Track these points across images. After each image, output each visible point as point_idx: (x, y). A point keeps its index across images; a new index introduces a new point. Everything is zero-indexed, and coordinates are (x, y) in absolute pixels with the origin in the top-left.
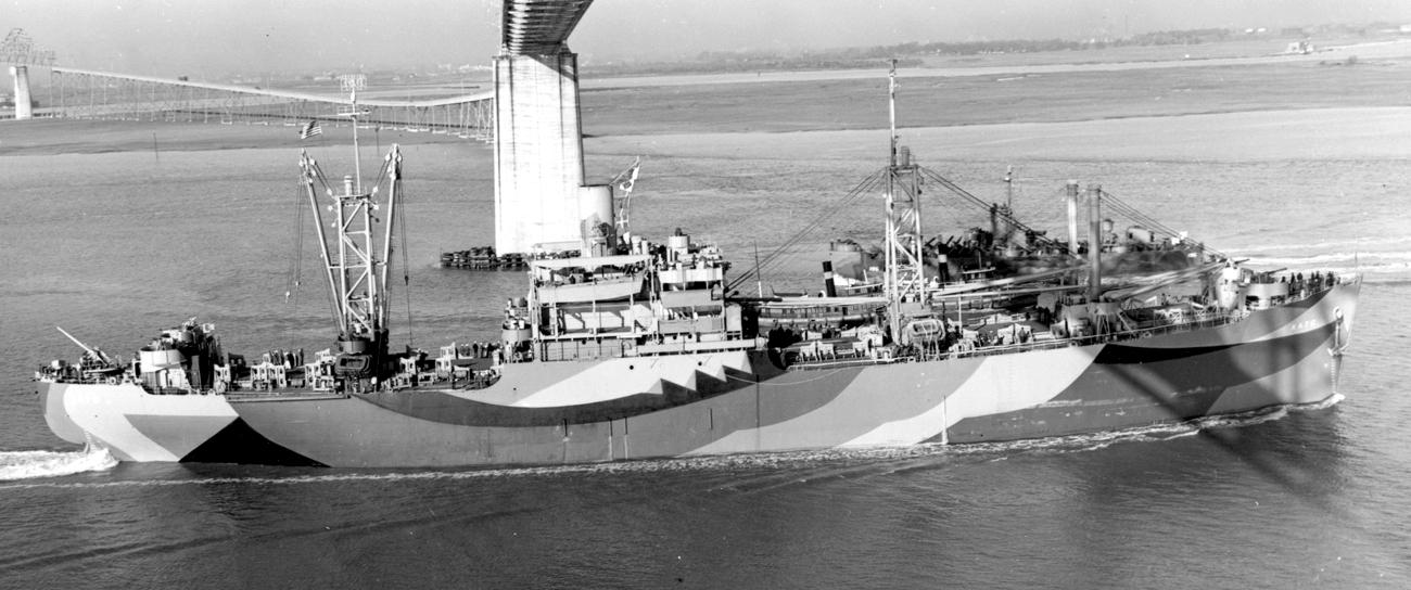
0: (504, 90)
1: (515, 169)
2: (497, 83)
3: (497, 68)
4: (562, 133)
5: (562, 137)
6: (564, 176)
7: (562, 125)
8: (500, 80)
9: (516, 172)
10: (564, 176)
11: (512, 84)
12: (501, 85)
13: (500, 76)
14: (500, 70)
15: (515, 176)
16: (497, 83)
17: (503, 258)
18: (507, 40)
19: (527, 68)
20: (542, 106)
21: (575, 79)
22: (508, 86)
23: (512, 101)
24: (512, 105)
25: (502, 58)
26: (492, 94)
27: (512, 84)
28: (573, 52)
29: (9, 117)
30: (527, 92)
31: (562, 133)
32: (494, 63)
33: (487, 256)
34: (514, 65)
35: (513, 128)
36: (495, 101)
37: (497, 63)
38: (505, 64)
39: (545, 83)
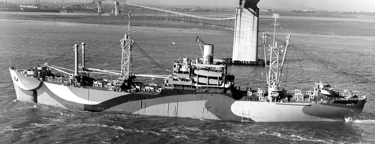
0: (239, 17)
1: (239, 38)
2: (237, 15)
3: (237, 11)
6: (253, 41)
7: (253, 27)
8: (238, 14)
9: (240, 39)
10: (253, 41)
11: (241, 15)
13: (238, 13)
14: (238, 11)
15: (239, 40)
16: (237, 15)
18: (241, 4)
19: (245, 11)
20: (248, 22)
21: (258, 16)
22: (240, 16)
25: (239, 8)
26: (236, 18)
27: (241, 15)
29: (114, 15)
30: (245, 18)
32: (237, 9)
33: (230, 61)
35: (240, 27)
36: (236, 20)
37: (237, 9)
38: (239, 10)
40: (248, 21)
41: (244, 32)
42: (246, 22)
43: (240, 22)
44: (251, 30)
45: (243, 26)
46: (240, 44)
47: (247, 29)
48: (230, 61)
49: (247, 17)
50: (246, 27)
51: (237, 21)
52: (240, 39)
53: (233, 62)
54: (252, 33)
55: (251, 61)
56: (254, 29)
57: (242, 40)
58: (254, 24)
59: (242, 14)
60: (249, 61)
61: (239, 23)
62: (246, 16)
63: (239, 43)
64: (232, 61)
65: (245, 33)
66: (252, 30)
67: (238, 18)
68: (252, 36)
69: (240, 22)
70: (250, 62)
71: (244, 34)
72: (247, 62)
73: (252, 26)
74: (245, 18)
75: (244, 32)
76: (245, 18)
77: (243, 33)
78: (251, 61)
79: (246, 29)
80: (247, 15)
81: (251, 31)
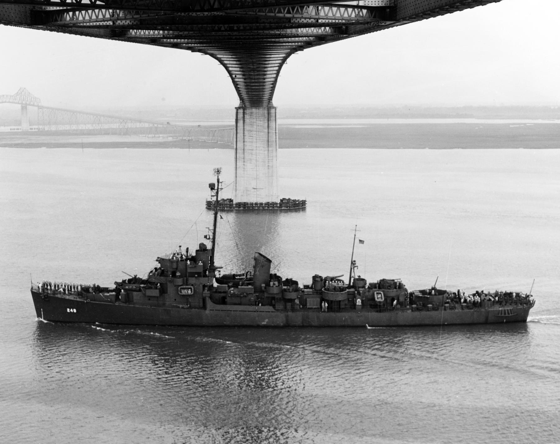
0: (240, 123)
4: (268, 145)
5: (268, 147)
9: (245, 163)
10: (268, 166)
11: (244, 121)
12: (239, 121)
13: (239, 116)
14: (239, 114)
17: (236, 204)
20: (259, 132)
23: (244, 129)
24: (244, 131)
27: (244, 121)
28: (275, 106)
29: (18, 129)
30: (251, 125)
31: (268, 145)
34: (245, 111)
35: (244, 142)
39: (260, 121)
40: (258, 130)
41: (253, 150)
42: (255, 133)
43: (244, 133)
44: (265, 146)
45: (251, 140)
46: (245, 172)
47: (257, 145)
48: (228, 203)
49: (255, 123)
50: (255, 140)
51: (238, 131)
52: (245, 163)
53: (234, 205)
54: (266, 152)
55: (268, 203)
56: (269, 144)
57: (249, 166)
58: (269, 134)
59: (245, 117)
60: (264, 203)
61: (242, 135)
62: (254, 122)
63: (244, 171)
64: (233, 204)
65: (254, 152)
66: (266, 146)
67: (239, 125)
68: (267, 157)
69: (244, 133)
70: (265, 204)
71: (252, 154)
72: (261, 204)
73: (266, 139)
74: (252, 125)
75: (253, 150)
76: (252, 125)
77: (250, 151)
78: (268, 201)
79: (255, 145)
80: (255, 120)
81: (264, 147)
